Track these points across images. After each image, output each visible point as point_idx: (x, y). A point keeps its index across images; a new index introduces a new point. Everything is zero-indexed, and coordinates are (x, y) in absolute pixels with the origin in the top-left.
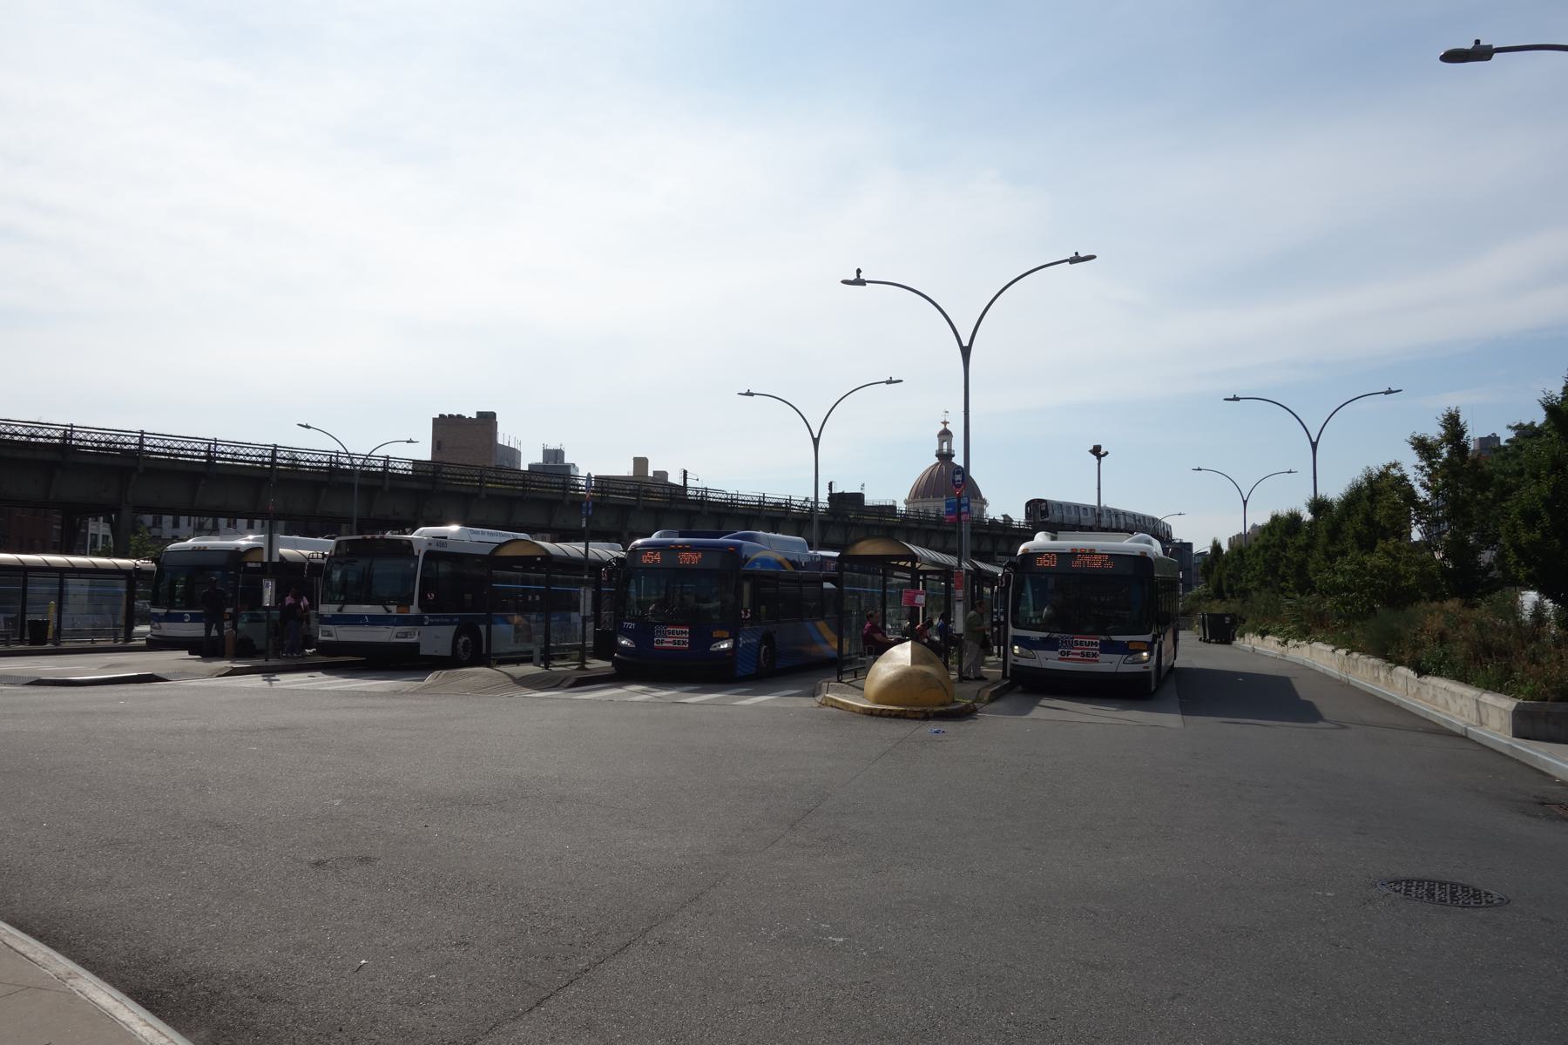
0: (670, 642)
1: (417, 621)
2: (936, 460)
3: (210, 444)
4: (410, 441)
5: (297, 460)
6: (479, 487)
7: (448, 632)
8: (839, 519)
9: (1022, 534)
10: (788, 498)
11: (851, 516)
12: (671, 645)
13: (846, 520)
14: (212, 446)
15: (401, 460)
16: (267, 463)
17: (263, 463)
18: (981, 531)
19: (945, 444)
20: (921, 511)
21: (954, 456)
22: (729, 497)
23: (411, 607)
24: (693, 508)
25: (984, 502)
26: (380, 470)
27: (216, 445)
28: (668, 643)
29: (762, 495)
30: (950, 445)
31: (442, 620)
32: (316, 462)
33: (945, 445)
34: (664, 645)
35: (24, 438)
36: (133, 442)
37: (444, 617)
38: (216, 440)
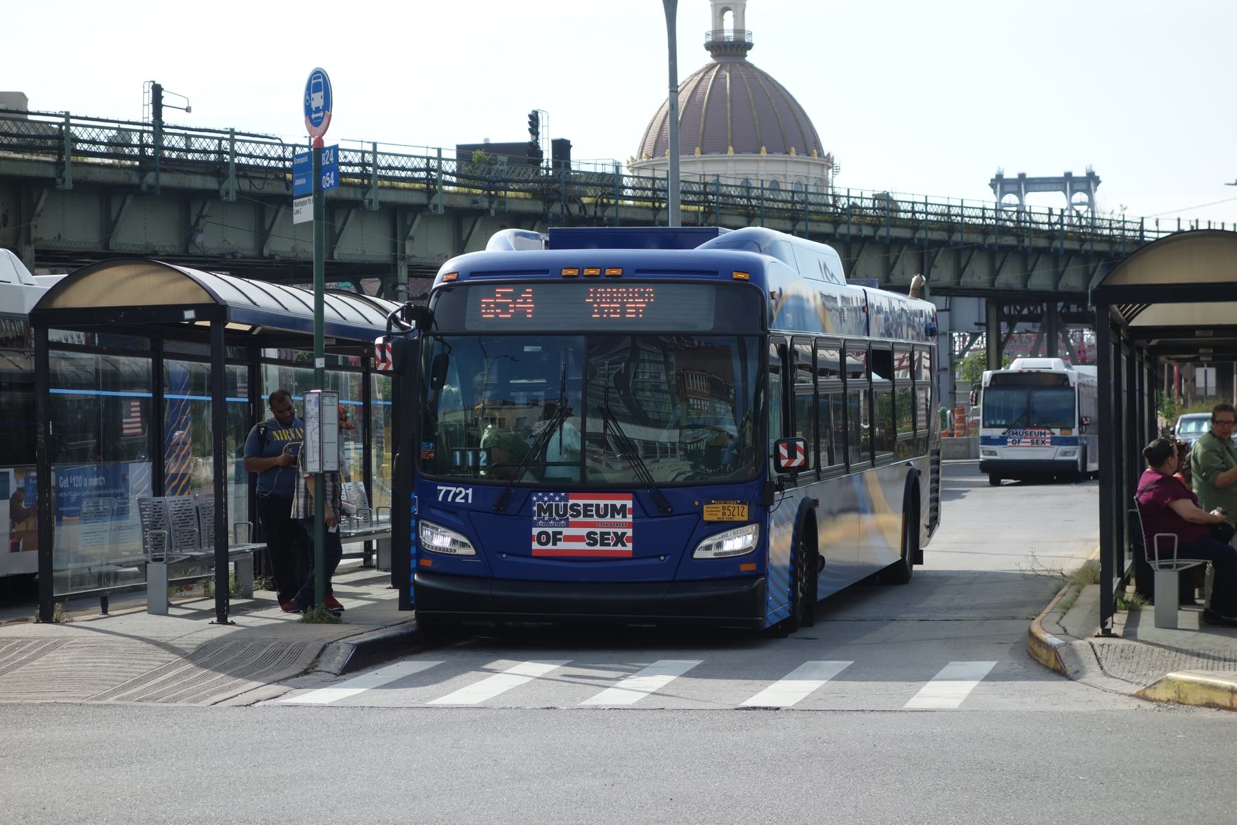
2: (707, 58)
8: (556, 208)
9: (992, 239)
10: (434, 154)
11: (586, 200)
13: (575, 209)
18: (896, 232)
19: (729, 19)
20: (754, 184)
21: (749, 46)
22: (288, 154)
24: (197, 182)
25: (827, 162)
29: (370, 148)
30: (740, 18)
33: (729, 19)
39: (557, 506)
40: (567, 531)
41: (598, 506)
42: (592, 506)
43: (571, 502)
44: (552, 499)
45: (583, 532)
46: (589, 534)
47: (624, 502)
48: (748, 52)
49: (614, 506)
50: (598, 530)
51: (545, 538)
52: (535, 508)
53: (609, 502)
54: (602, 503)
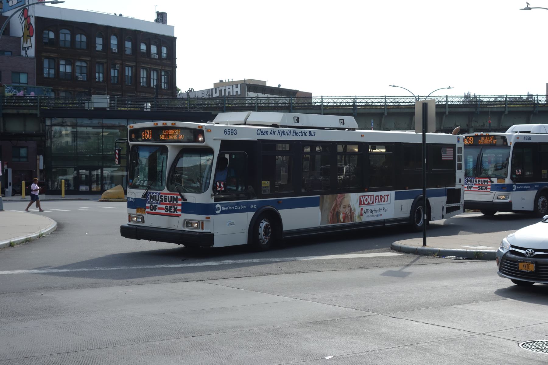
1: (509, 188)
3: (354, 99)
4: (449, 88)
5: (398, 102)
6: (505, 107)
7: (532, 194)
14: (355, 99)
15: (456, 97)
16: (382, 106)
17: (380, 106)
23: (506, 179)
26: (443, 103)
27: (356, 99)
31: (526, 187)
32: (408, 103)
35: (273, 105)
36: (319, 102)
37: (527, 185)
38: (356, 97)
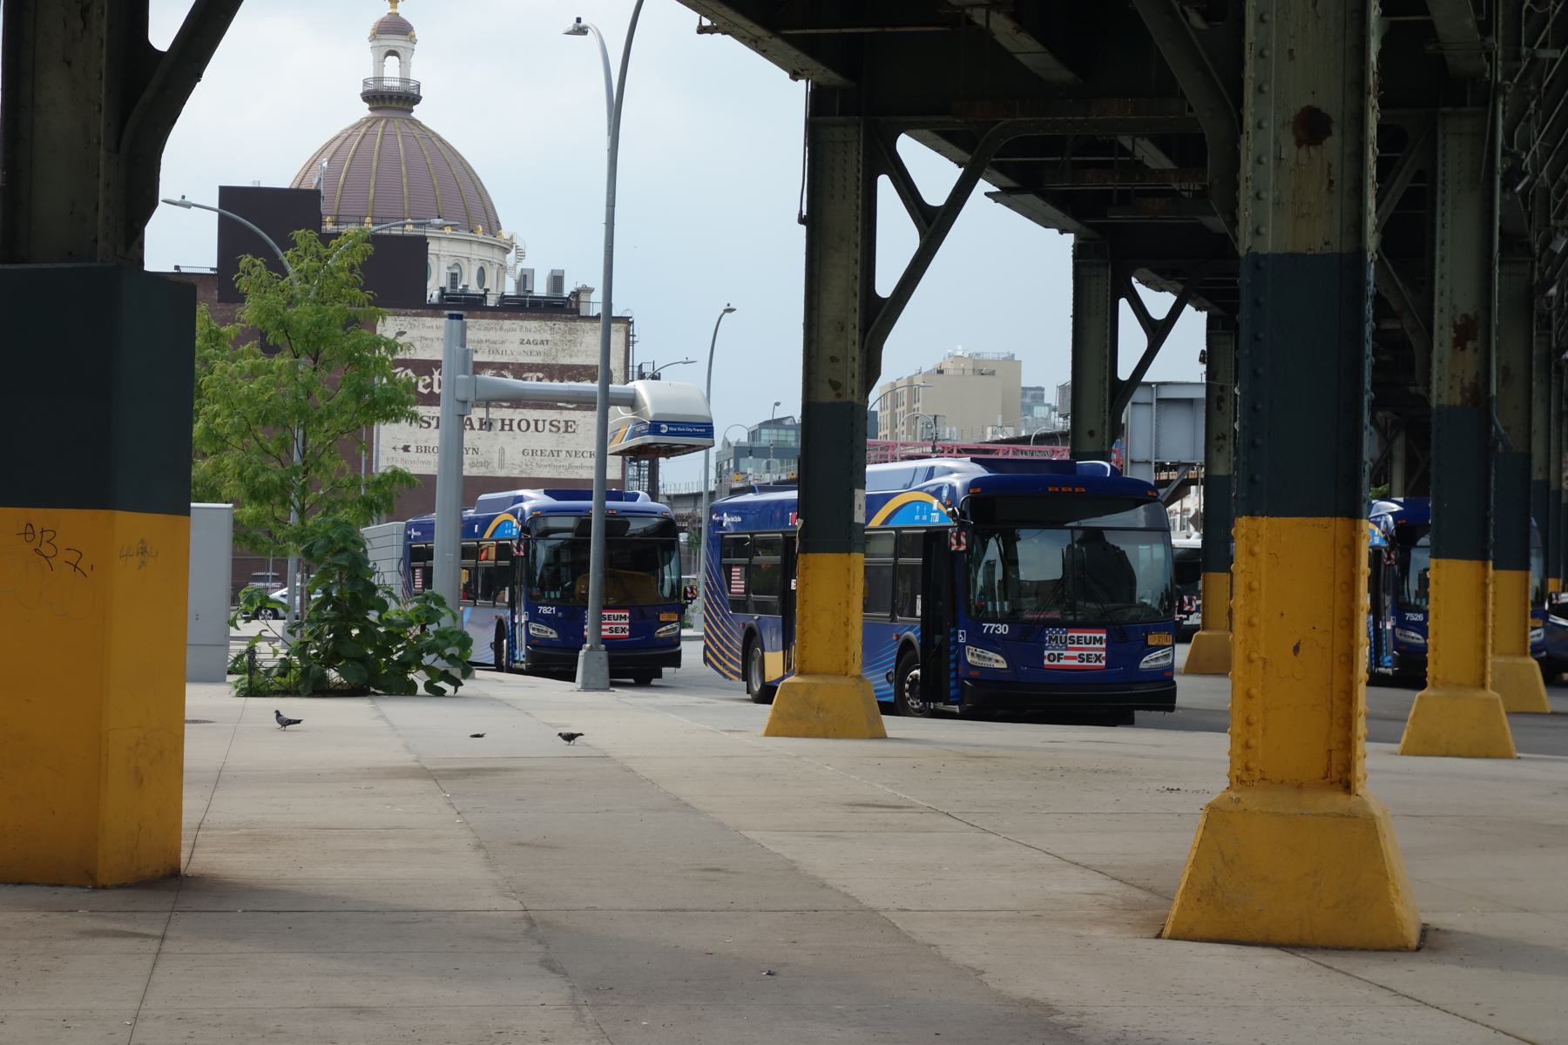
0: (1073, 658)
12: (1075, 663)
28: (1069, 658)
34: (1063, 662)
39: (1061, 637)
40: (1066, 653)
41: (1086, 637)
42: (1081, 637)
43: (1069, 635)
44: (1057, 632)
45: (1076, 653)
46: (1080, 655)
47: (1101, 635)
48: (414, 107)
49: (1095, 638)
50: (1085, 653)
51: (1052, 657)
52: (1047, 638)
53: (1093, 635)
54: (1088, 635)
